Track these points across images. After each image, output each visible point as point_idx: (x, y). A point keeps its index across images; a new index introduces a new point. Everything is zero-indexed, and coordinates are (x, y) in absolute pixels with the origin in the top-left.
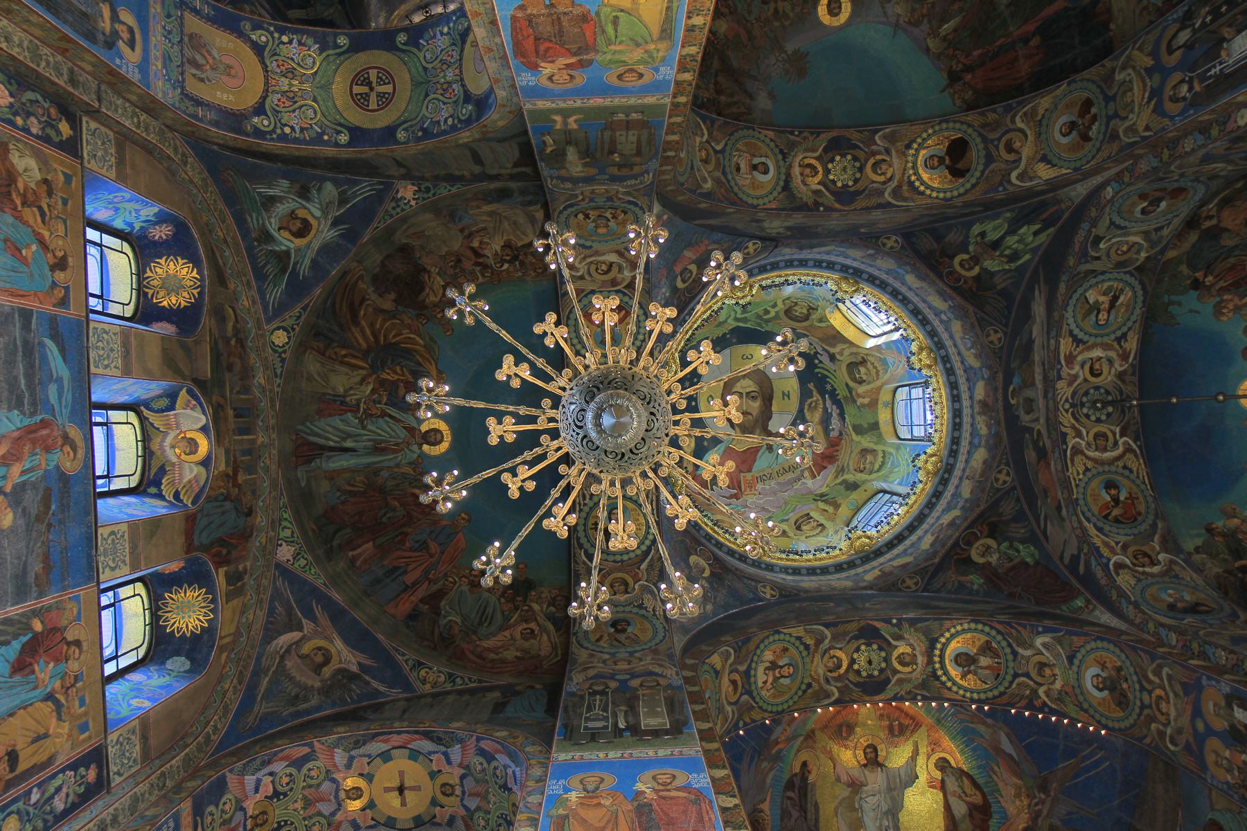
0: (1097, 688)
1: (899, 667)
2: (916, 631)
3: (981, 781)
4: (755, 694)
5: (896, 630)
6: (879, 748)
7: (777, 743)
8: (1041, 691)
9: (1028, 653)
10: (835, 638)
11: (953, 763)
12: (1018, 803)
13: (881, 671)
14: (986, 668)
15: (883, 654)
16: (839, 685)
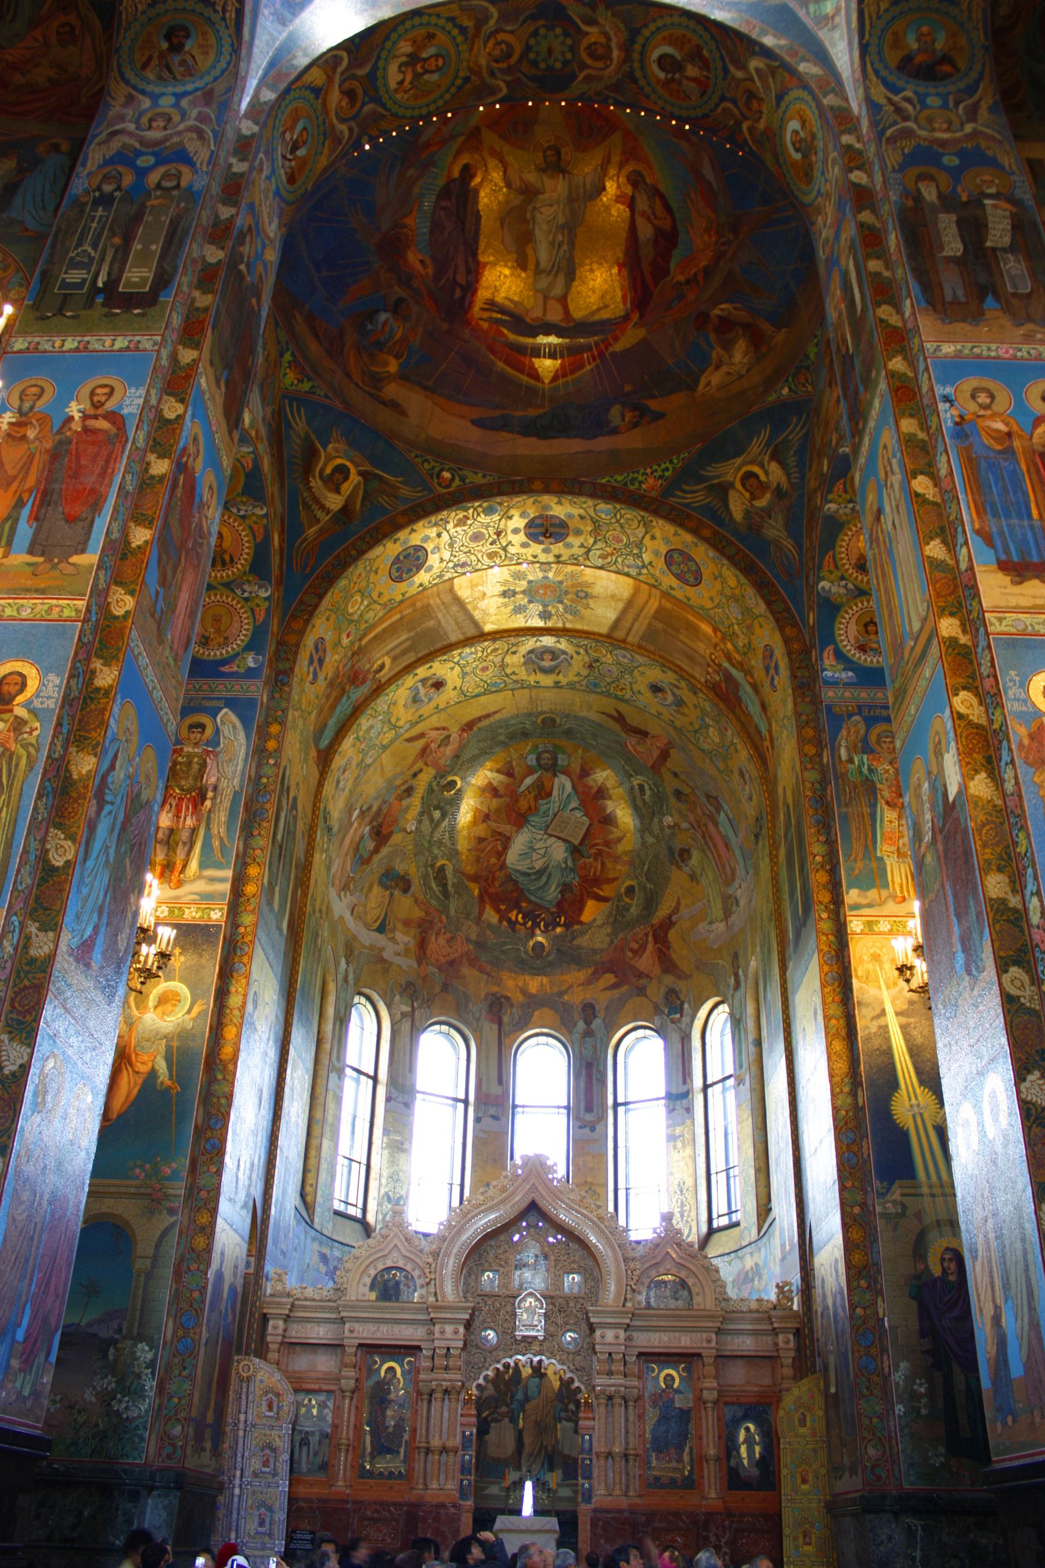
0: (794, 145)
1: (589, 61)
2: (613, 15)
3: (674, 205)
4: (385, 99)
5: (588, 11)
6: (563, 151)
7: (429, 145)
8: (745, 126)
9: (740, 74)
10: (503, 17)
11: (648, 180)
12: (706, 237)
13: (566, 63)
14: (694, 80)
15: (569, 41)
16: (508, 78)
